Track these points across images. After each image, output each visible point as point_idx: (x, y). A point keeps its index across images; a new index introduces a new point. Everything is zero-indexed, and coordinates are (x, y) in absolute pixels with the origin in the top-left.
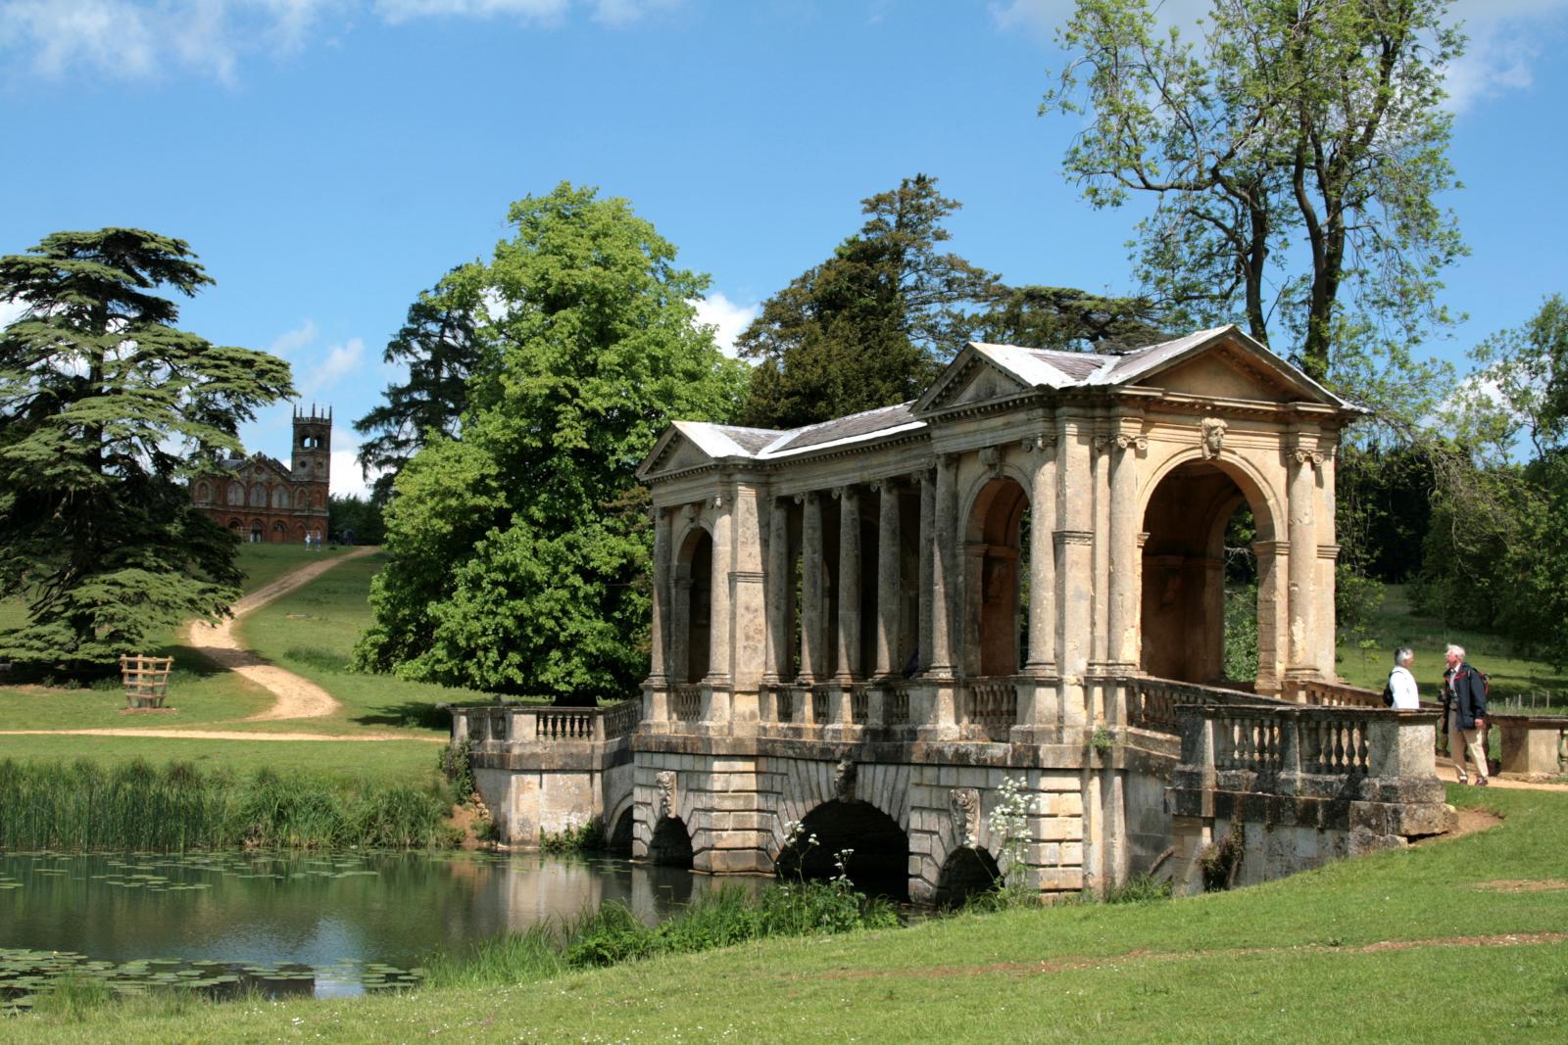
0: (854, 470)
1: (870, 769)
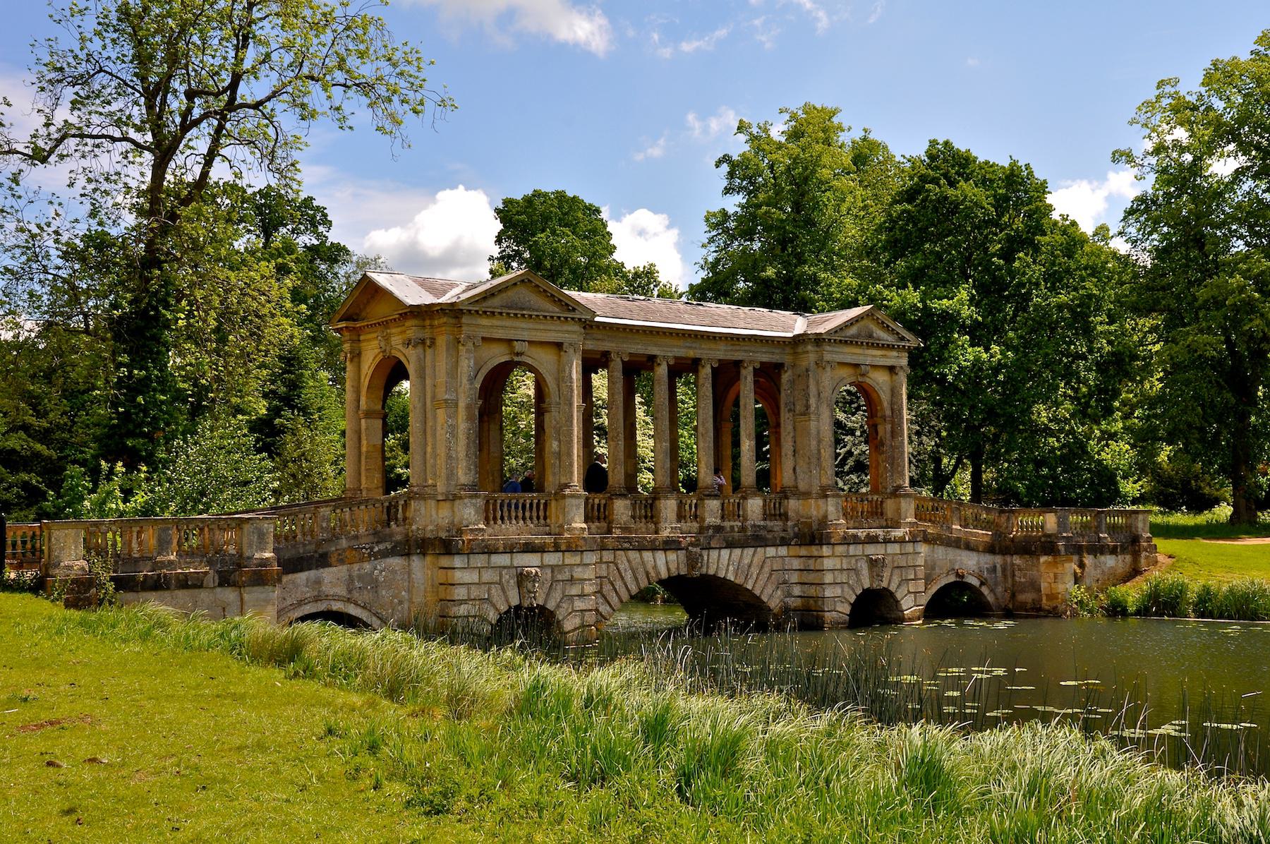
0: (680, 347)
1: (714, 554)
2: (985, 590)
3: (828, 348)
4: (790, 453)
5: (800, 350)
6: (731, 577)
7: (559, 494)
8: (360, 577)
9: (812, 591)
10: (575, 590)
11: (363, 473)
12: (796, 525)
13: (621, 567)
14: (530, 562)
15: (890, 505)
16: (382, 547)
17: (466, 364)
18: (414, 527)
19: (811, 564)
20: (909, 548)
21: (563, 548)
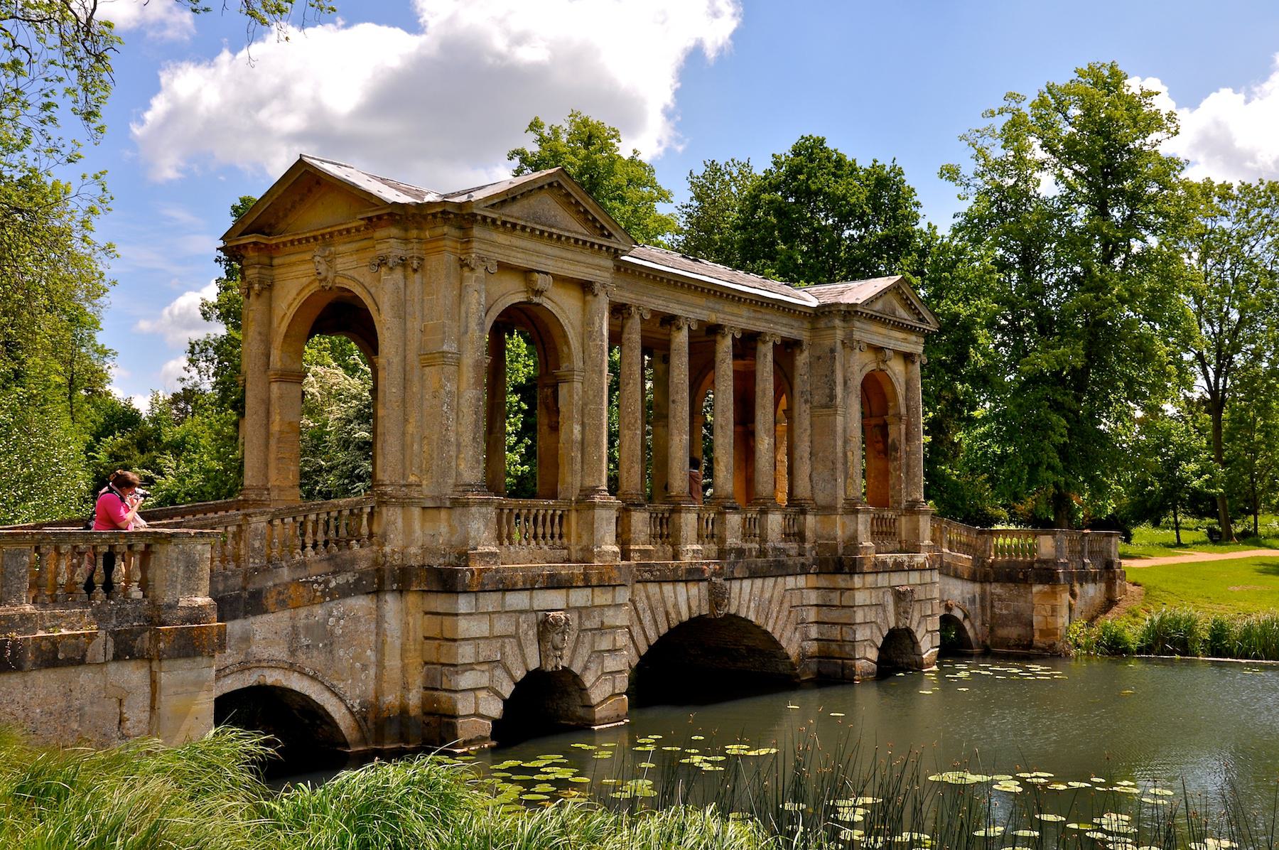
1: (736, 585)
2: (967, 625)
3: (858, 324)
4: (807, 455)
5: (822, 324)
6: (752, 617)
7: (585, 500)
8: (309, 629)
9: (835, 633)
10: (605, 644)
11: (272, 465)
12: (813, 548)
13: (640, 606)
14: (552, 600)
15: (904, 523)
16: (341, 580)
17: (475, 300)
18: (387, 549)
19: (835, 598)
20: (927, 576)
21: (594, 582)
